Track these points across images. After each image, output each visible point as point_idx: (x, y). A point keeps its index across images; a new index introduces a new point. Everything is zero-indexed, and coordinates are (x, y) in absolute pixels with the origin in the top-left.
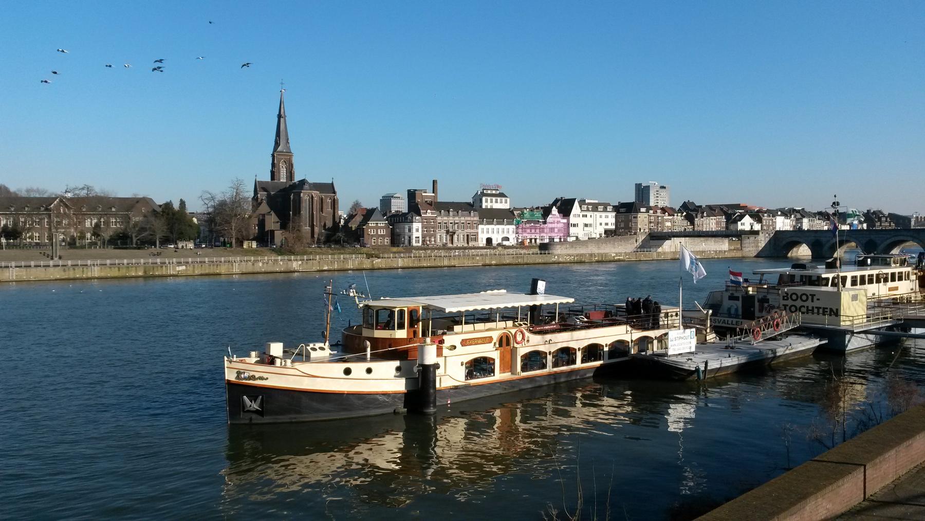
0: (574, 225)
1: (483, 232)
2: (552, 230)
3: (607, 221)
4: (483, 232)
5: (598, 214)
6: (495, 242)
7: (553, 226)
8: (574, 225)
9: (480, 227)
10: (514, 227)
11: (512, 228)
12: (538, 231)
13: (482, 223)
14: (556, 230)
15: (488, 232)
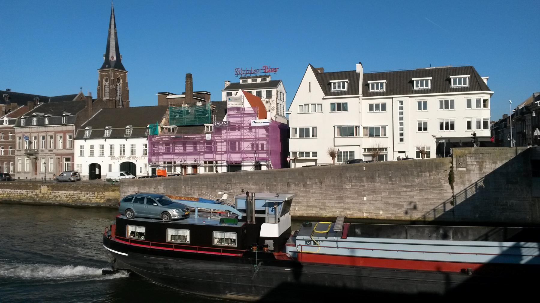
0: (304, 133)
1: (82, 154)
2: (234, 146)
3: (447, 115)
4: (82, 154)
5: (410, 102)
6: (105, 173)
7: (234, 135)
8: (304, 133)
9: (78, 143)
10: (145, 141)
11: (141, 143)
12: (200, 148)
13: (80, 136)
14: (246, 146)
15: (92, 153)
